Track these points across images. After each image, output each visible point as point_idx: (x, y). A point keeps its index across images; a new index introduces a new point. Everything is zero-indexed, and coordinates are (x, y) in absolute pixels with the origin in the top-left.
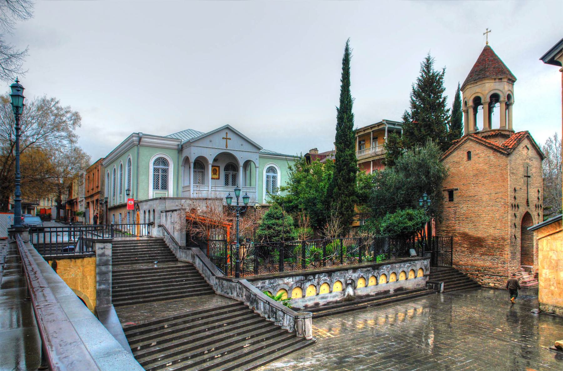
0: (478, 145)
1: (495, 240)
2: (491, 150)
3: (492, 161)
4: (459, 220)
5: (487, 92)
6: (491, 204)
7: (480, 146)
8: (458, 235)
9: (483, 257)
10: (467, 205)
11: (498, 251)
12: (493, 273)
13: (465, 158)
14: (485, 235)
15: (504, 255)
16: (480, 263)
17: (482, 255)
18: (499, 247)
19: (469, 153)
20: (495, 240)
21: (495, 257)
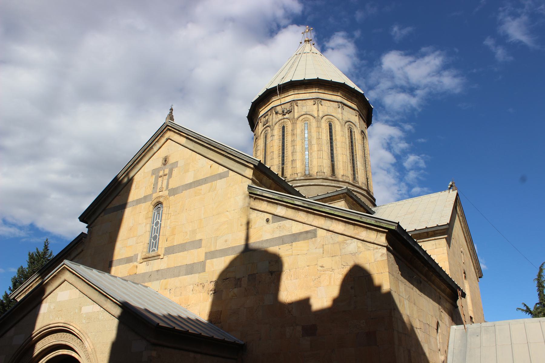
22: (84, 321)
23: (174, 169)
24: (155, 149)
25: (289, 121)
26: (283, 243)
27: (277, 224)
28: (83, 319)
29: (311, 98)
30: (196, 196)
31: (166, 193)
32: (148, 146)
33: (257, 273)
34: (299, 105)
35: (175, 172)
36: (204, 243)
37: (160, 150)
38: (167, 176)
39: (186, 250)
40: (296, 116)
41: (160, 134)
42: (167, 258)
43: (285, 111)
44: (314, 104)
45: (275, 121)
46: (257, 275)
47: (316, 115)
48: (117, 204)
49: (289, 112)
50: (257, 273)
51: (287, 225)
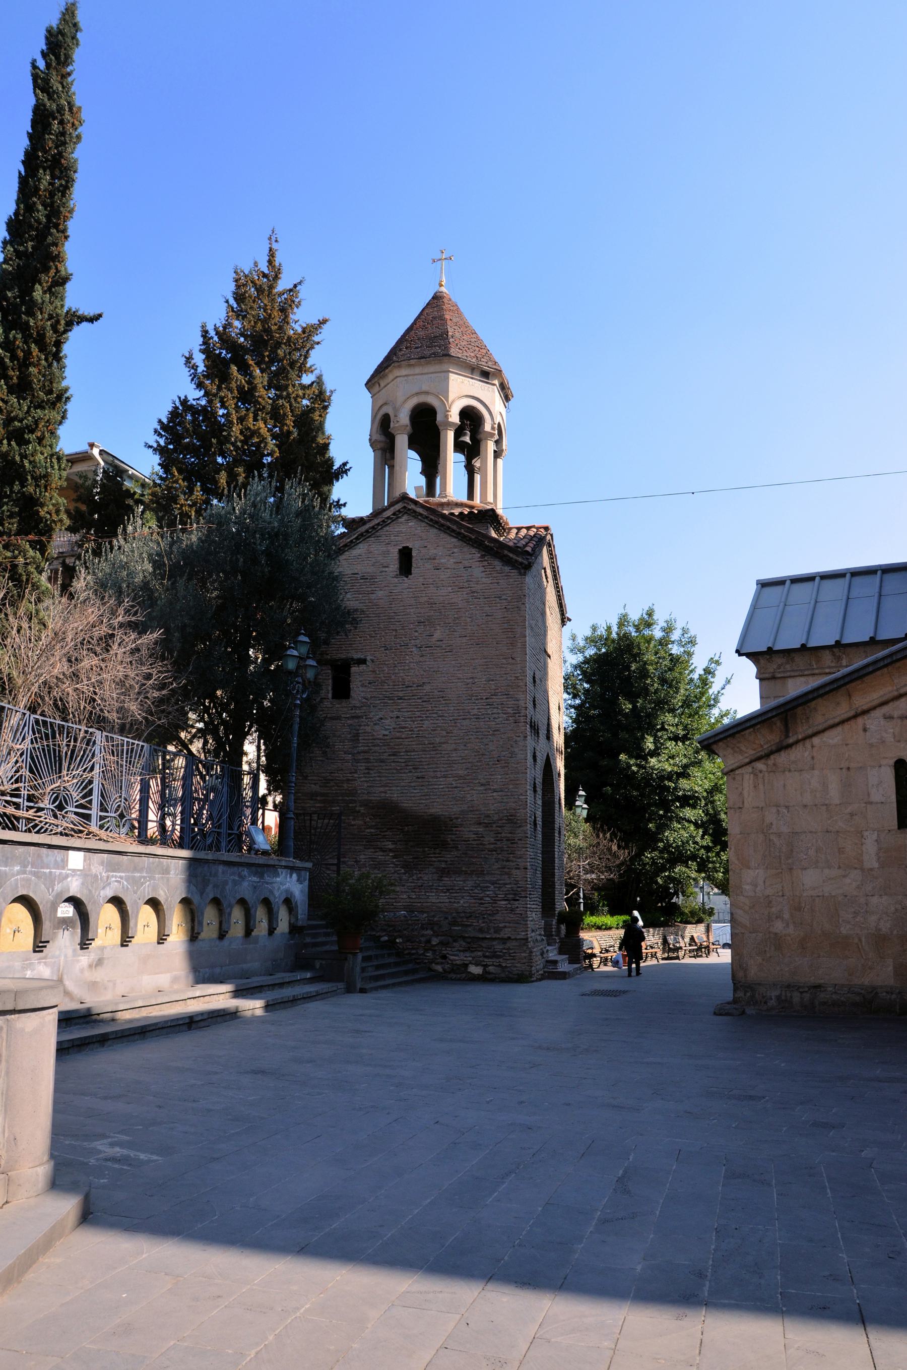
0: (434, 531)
1: (487, 825)
2: (474, 551)
4: (367, 760)
6: (475, 712)
7: (442, 535)
8: (362, 810)
9: (447, 881)
10: (396, 713)
12: (481, 930)
13: (394, 566)
14: (456, 809)
15: (514, 872)
16: (437, 899)
17: (444, 872)
18: (499, 844)
19: (406, 556)
20: (487, 825)
21: (487, 878)
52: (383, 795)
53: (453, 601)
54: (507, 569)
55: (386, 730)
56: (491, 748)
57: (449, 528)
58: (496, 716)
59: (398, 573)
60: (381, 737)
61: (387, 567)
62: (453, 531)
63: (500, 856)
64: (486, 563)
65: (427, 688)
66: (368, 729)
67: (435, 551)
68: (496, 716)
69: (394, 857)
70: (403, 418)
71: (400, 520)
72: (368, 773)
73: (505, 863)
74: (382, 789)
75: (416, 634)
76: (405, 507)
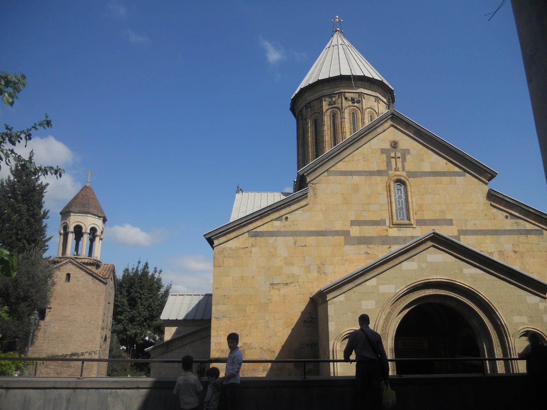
3: (90, 286)
4: (48, 340)
5: (88, 224)
10: (60, 325)
11: (87, 371)
19: (68, 275)
22: (469, 280)
23: (406, 155)
24: (379, 130)
25: (358, 109)
26: (521, 234)
27: (514, 221)
28: (468, 278)
29: (374, 95)
30: (437, 184)
31: (404, 174)
32: (373, 126)
33: (504, 251)
34: (365, 97)
35: (408, 157)
36: (454, 222)
37: (384, 132)
38: (401, 158)
39: (438, 225)
40: (364, 108)
41: (385, 119)
42: (420, 228)
43: (356, 100)
44: (375, 102)
45: (345, 106)
46: (504, 252)
47: (377, 112)
48: (344, 169)
49: (358, 102)
50: (504, 251)
51: (521, 223)
52: (52, 351)
53: (82, 291)
54: (100, 283)
55: (56, 330)
56: (89, 337)
57: (83, 269)
58: (91, 327)
59: (65, 281)
60: (54, 332)
61: (62, 279)
62: (85, 270)
63: (88, 370)
64: (93, 280)
65: (71, 317)
66: (50, 329)
67: (78, 275)
68: (91, 327)
69: (54, 371)
70: (71, 229)
71: (68, 264)
72: (48, 344)
73: (89, 372)
74: (52, 349)
75: (69, 300)
76: (70, 261)
